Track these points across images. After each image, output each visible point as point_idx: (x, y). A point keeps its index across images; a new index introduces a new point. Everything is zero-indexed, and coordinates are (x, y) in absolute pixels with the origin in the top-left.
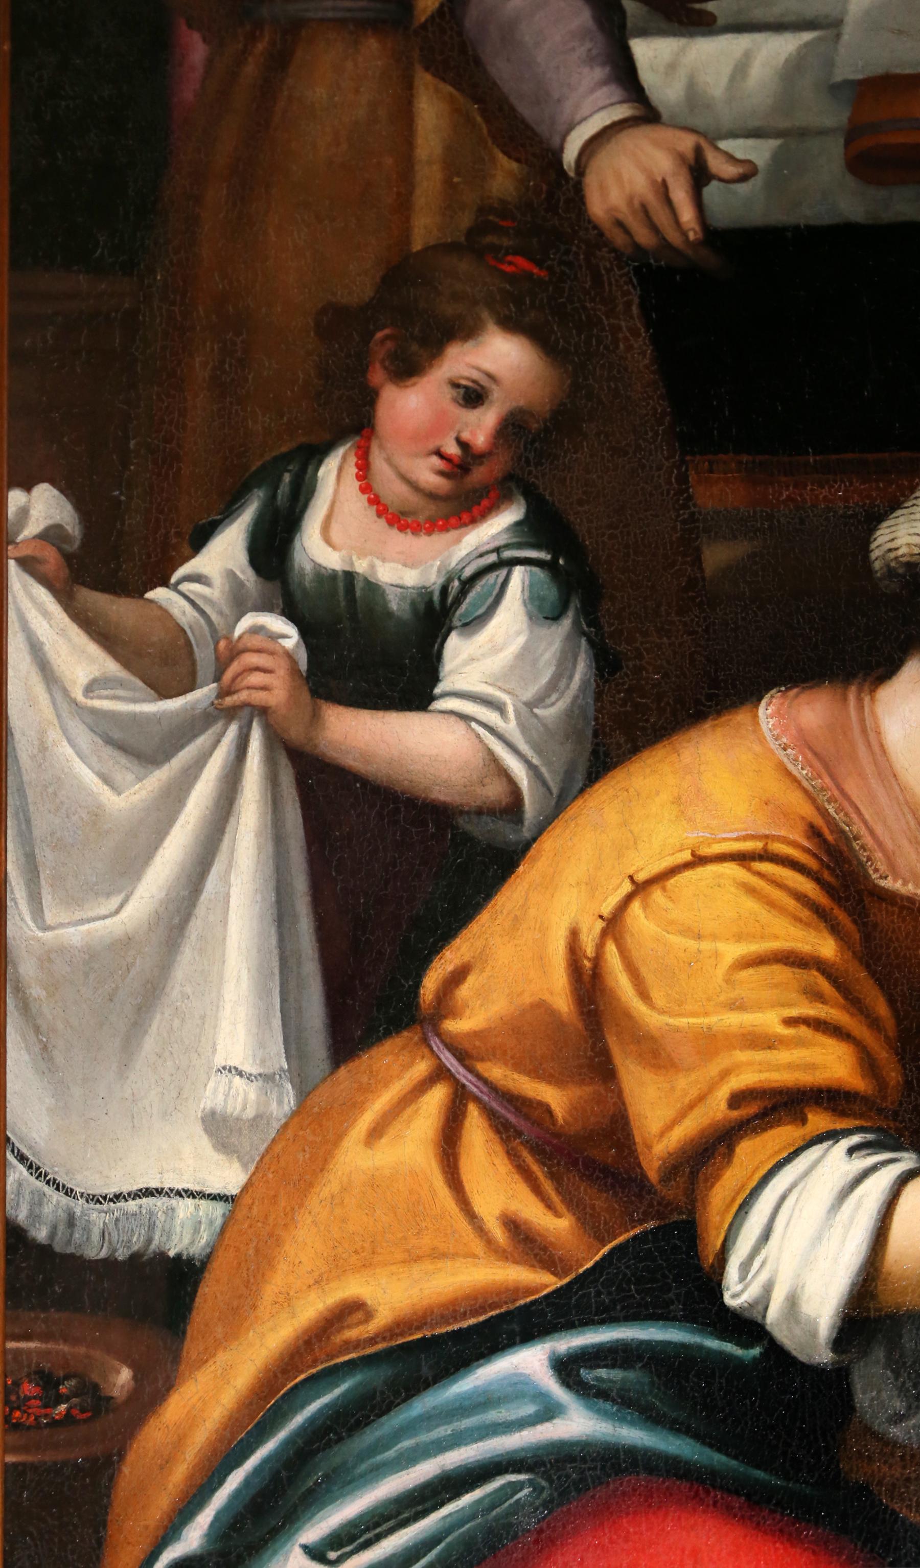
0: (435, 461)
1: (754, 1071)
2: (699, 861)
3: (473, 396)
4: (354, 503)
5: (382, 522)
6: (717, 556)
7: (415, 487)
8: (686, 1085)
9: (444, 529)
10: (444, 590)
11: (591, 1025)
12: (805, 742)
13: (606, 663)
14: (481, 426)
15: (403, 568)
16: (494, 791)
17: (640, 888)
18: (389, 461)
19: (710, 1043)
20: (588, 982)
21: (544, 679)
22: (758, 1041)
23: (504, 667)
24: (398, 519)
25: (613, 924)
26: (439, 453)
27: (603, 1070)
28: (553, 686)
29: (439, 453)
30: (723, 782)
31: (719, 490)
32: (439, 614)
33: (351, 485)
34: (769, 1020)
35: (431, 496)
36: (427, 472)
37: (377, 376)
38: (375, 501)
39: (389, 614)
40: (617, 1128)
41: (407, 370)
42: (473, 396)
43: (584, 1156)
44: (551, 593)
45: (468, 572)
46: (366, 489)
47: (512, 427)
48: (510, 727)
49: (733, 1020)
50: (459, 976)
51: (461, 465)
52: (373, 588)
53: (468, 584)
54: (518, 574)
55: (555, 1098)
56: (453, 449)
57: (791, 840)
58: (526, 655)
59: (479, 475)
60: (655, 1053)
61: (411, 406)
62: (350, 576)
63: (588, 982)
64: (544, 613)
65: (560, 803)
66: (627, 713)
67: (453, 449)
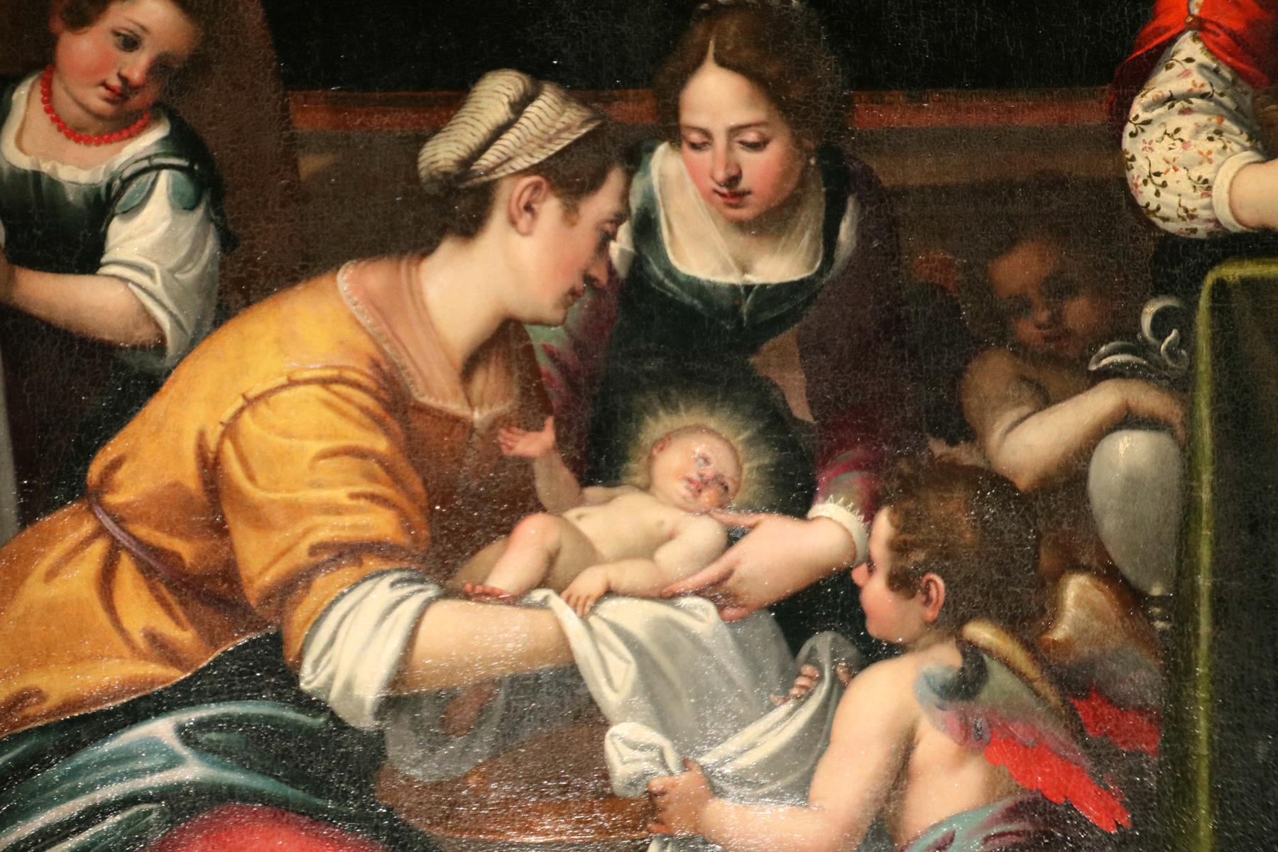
0: (102, 90)
1: (329, 530)
2: (292, 383)
3: (130, 43)
4: (40, 121)
5: (62, 135)
6: (310, 164)
7: (87, 110)
8: (278, 539)
9: (109, 141)
10: (109, 186)
11: (213, 496)
12: (371, 301)
13: (228, 241)
14: (136, 65)
15: (78, 170)
16: (144, 334)
17: (251, 402)
18: (66, 89)
19: (296, 510)
20: (210, 466)
21: (183, 252)
22: (334, 509)
23: (153, 243)
24: (75, 133)
25: (230, 430)
26: (104, 84)
27: (221, 530)
28: (189, 257)
29: (104, 84)
30: (312, 329)
31: (311, 118)
32: (105, 204)
33: (38, 107)
34: (340, 495)
35: (99, 116)
36: (96, 100)
37: (57, 25)
38: (56, 119)
39: (68, 204)
40: (230, 573)
41: (81, 20)
42: (130, 43)
43: (206, 590)
44: (188, 190)
45: (127, 174)
46: (49, 110)
47: (160, 66)
48: (157, 287)
49: (314, 495)
50: (116, 464)
51: (122, 93)
52: (55, 184)
53: (126, 182)
54: (164, 176)
55: (185, 549)
56: (115, 82)
57: (359, 370)
58: (169, 240)
59: (136, 101)
60: (258, 519)
61: (83, 49)
62: (37, 175)
63: (210, 466)
64: (184, 204)
65: (191, 345)
66: (240, 280)
67: (115, 82)
